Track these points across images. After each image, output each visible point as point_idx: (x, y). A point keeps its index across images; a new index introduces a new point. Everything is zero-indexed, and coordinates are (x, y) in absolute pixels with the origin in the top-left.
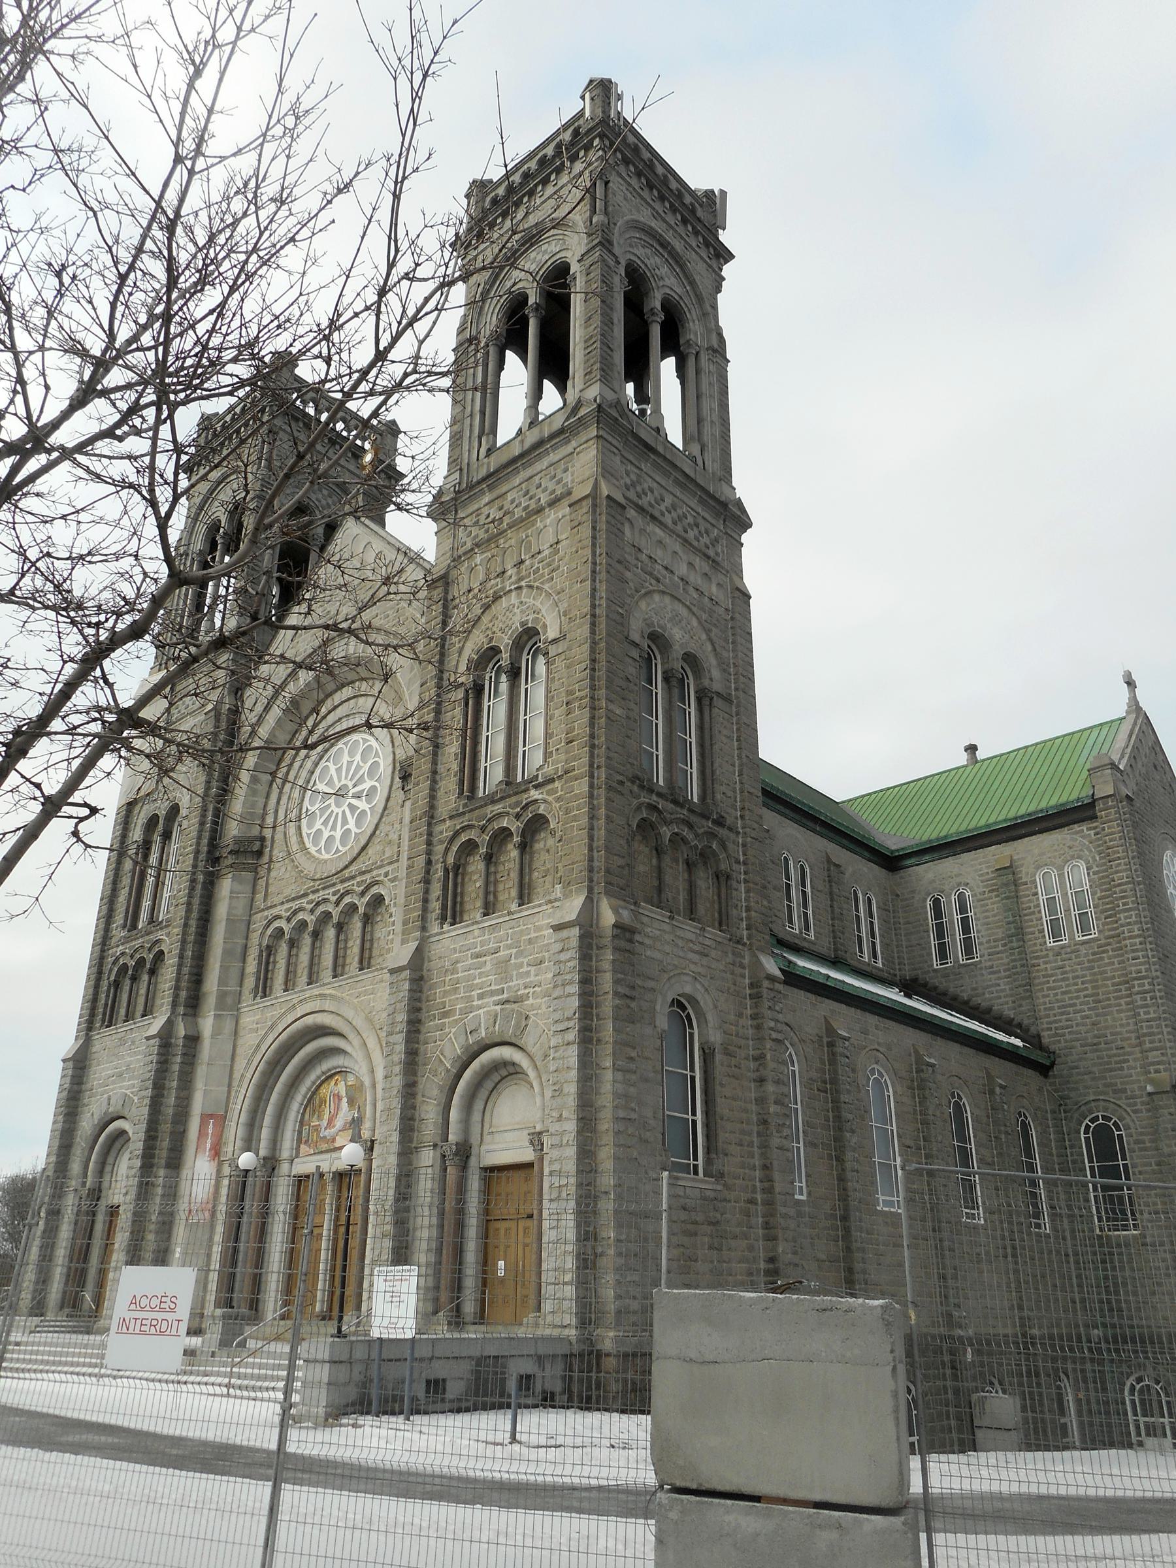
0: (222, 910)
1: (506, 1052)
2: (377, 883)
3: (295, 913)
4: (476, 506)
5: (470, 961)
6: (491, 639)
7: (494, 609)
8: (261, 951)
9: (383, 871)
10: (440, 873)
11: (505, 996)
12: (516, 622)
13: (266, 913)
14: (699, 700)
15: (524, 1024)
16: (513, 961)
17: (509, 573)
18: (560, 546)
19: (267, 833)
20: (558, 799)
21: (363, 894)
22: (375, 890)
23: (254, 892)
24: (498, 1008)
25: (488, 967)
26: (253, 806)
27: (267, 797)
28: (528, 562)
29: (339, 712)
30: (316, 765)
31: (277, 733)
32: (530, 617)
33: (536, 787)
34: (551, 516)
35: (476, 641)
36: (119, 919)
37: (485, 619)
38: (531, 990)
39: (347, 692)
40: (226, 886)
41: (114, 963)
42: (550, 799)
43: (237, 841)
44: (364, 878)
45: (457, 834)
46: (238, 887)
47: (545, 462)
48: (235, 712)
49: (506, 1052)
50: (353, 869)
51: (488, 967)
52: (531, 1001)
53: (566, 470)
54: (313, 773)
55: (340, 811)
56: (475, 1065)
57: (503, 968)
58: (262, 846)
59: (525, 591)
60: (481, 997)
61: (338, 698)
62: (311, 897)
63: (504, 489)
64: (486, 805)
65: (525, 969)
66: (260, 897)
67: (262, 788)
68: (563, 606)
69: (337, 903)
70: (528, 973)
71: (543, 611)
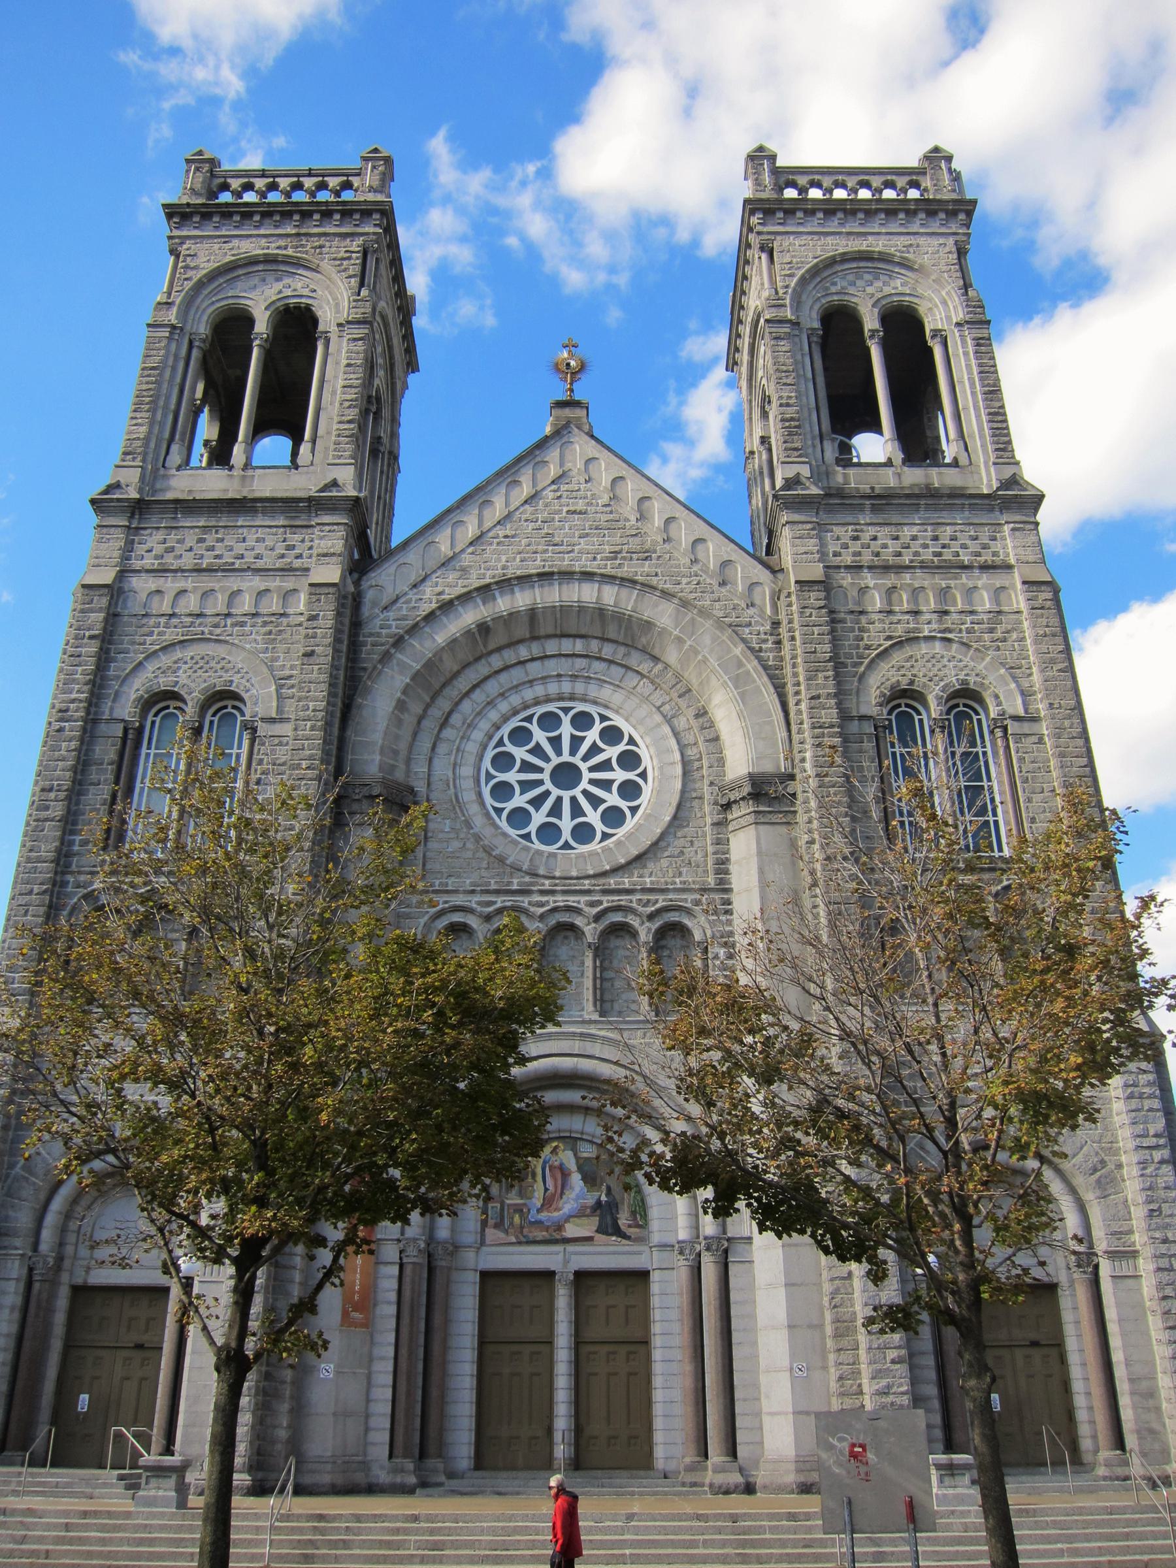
7: (908, 650)
12: (953, 680)
19: (420, 787)
22: (673, 917)
29: (552, 667)
30: (506, 719)
31: (445, 657)
37: (897, 657)
39: (567, 646)
44: (652, 897)
53: (994, 539)
54: (498, 728)
61: (551, 647)
62: (537, 898)
67: (409, 720)
69: (597, 918)
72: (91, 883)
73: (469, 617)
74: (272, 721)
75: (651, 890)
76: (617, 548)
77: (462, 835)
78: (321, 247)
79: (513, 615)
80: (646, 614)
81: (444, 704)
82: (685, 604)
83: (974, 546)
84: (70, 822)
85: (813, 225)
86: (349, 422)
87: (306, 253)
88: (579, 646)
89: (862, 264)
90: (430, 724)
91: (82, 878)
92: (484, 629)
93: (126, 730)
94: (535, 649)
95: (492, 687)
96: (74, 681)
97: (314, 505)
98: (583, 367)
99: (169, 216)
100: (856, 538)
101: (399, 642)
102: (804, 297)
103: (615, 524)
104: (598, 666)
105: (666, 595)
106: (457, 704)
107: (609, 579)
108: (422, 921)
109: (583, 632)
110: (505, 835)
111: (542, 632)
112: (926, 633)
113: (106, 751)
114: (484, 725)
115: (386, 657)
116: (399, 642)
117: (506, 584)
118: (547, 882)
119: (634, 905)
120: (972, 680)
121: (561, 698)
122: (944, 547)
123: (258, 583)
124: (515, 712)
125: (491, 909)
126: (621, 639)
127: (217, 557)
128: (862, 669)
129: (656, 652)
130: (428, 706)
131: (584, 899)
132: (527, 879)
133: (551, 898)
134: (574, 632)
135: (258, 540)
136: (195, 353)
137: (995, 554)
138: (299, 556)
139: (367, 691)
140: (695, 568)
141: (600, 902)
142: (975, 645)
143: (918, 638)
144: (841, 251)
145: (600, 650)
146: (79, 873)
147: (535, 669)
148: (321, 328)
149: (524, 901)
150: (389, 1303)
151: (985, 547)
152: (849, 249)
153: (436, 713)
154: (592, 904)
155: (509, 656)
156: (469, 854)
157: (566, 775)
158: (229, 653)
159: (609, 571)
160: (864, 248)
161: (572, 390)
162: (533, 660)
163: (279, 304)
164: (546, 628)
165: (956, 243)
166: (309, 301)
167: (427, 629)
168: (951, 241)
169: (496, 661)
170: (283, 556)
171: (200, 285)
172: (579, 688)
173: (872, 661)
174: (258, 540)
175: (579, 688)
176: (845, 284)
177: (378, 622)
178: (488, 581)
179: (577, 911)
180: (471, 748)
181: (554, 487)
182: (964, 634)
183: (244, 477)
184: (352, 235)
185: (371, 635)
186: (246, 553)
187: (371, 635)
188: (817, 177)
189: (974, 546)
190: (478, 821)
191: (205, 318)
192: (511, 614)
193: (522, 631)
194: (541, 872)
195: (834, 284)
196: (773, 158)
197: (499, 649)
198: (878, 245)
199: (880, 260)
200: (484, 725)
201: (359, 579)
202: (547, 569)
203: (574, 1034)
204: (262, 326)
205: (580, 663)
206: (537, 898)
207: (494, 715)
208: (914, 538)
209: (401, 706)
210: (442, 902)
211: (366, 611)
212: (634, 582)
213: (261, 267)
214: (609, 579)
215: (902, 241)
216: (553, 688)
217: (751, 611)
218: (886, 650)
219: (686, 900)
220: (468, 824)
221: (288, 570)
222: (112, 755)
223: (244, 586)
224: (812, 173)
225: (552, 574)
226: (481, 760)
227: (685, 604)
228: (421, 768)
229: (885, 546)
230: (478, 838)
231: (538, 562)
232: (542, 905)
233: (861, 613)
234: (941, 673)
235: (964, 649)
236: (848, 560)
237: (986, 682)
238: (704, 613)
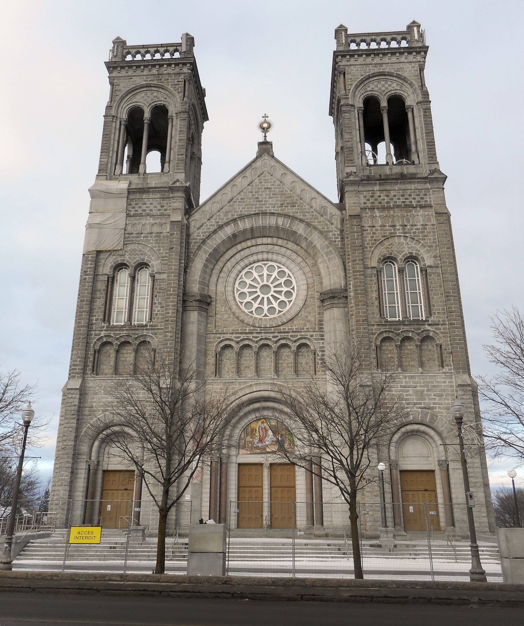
1: (423, 428)
2: (306, 338)
3: (243, 340)
4: (371, 189)
5: (400, 389)
6: (391, 254)
7: (391, 241)
9: (309, 334)
10: (374, 348)
11: (423, 406)
12: (406, 251)
13: (218, 335)
15: (436, 418)
16: (425, 392)
17: (398, 227)
18: (427, 227)
19: (213, 296)
20: (442, 333)
21: (295, 341)
22: (303, 341)
24: (420, 410)
25: (411, 392)
26: (204, 278)
27: (210, 276)
28: (409, 227)
29: (260, 248)
30: (243, 269)
33: (429, 325)
34: (421, 212)
36: (98, 314)
37: (386, 243)
38: (438, 406)
39: (265, 240)
40: (194, 316)
41: (98, 340)
42: (438, 332)
43: (201, 295)
44: (296, 334)
45: (382, 332)
46: (201, 319)
47: (413, 186)
48: (188, 227)
49: (423, 428)
50: (286, 328)
51: (411, 392)
52: (437, 410)
53: (426, 195)
54: (241, 272)
55: (265, 297)
56: (403, 430)
57: (420, 394)
59: (409, 239)
61: (259, 241)
62: (255, 335)
63: (388, 188)
64: (399, 325)
65: (433, 397)
66: (211, 327)
67: (208, 271)
70: (435, 399)
71: (422, 251)
72: (101, 334)
73: (229, 230)
74: (160, 273)
75: (295, 332)
76: (283, 202)
77: (229, 313)
78: (168, 80)
79: (245, 230)
80: (294, 228)
81: (220, 264)
82: (308, 224)
83: (418, 198)
84: (91, 312)
85: (361, 60)
86: (182, 155)
87: (162, 82)
88: (269, 240)
89: (380, 77)
90: (216, 271)
91: (97, 332)
92: (234, 236)
93: (108, 278)
94: (253, 242)
95: (238, 257)
96: (89, 260)
97: (172, 189)
98: (270, 126)
99: (108, 68)
100: (372, 197)
101: (204, 242)
102: (357, 93)
103: (282, 194)
104: (276, 248)
105: (301, 221)
106: (225, 264)
107: (279, 215)
108: (215, 344)
109: (271, 235)
110: (244, 312)
111: (256, 236)
112: (398, 234)
113: (101, 286)
114: (235, 271)
115: (199, 248)
116: (204, 242)
117: (242, 217)
118: (259, 329)
119: (289, 337)
120: (414, 252)
121: (263, 260)
122: (406, 199)
123: (151, 221)
124: (247, 266)
125: (239, 339)
126: (285, 238)
127: (136, 211)
128: (373, 249)
129: (298, 242)
130: (215, 265)
131: (271, 335)
132: (252, 328)
133: (260, 335)
134: (268, 235)
135: (151, 204)
136: (122, 127)
137: (427, 201)
138: (166, 210)
139: (193, 260)
140: (312, 210)
141: (278, 336)
142: (416, 238)
143: (395, 236)
144: (372, 72)
145: (277, 242)
146: (96, 330)
147: (253, 249)
148: (170, 114)
149: (251, 336)
150: (208, 475)
151: (422, 198)
152: (376, 71)
153: (218, 267)
154: (274, 337)
155: (244, 245)
156: (231, 319)
157: (265, 288)
158: (143, 248)
159: (280, 211)
160: (381, 70)
161: (265, 136)
162: (252, 246)
163: (153, 104)
164: (256, 234)
165: (419, 65)
166: (165, 103)
167: (214, 236)
168: (417, 65)
169: (239, 247)
170: (160, 210)
171: (123, 98)
172: (270, 256)
173: (377, 246)
174: (151, 204)
175: (270, 256)
176: (373, 86)
177: (196, 234)
178: (235, 216)
179: (270, 339)
180: (231, 280)
181: (259, 178)
182: (412, 234)
183: (144, 178)
184: (179, 74)
185: (194, 239)
186: (147, 209)
187: (194, 239)
188: (364, 38)
189: (418, 198)
190: (234, 307)
191: (125, 111)
192: (244, 230)
193: (249, 236)
194: (257, 325)
195: (369, 87)
196: (346, 30)
197: (240, 243)
198: (387, 69)
199: (387, 75)
200: (235, 271)
201: (189, 218)
202: (257, 212)
203: (269, 383)
204: (147, 115)
205: (270, 247)
206: (255, 335)
207: (239, 267)
208: (395, 196)
209: (205, 266)
211: (192, 229)
212: (289, 216)
213: (145, 89)
214: (279, 215)
215: (396, 66)
216: (260, 257)
217: (333, 226)
218: (382, 241)
219: (307, 335)
220: (230, 308)
221: (162, 215)
222: (104, 287)
223: (147, 222)
224: (362, 36)
225: (259, 213)
226: (235, 284)
227: (308, 224)
228: (212, 288)
229: (384, 199)
230: (234, 314)
231: (254, 209)
232: (256, 337)
233: (373, 227)
234: (402, 250)
235: (412, 240)
236: (369, 205)
237: (419, 253)
238: (315, 228)
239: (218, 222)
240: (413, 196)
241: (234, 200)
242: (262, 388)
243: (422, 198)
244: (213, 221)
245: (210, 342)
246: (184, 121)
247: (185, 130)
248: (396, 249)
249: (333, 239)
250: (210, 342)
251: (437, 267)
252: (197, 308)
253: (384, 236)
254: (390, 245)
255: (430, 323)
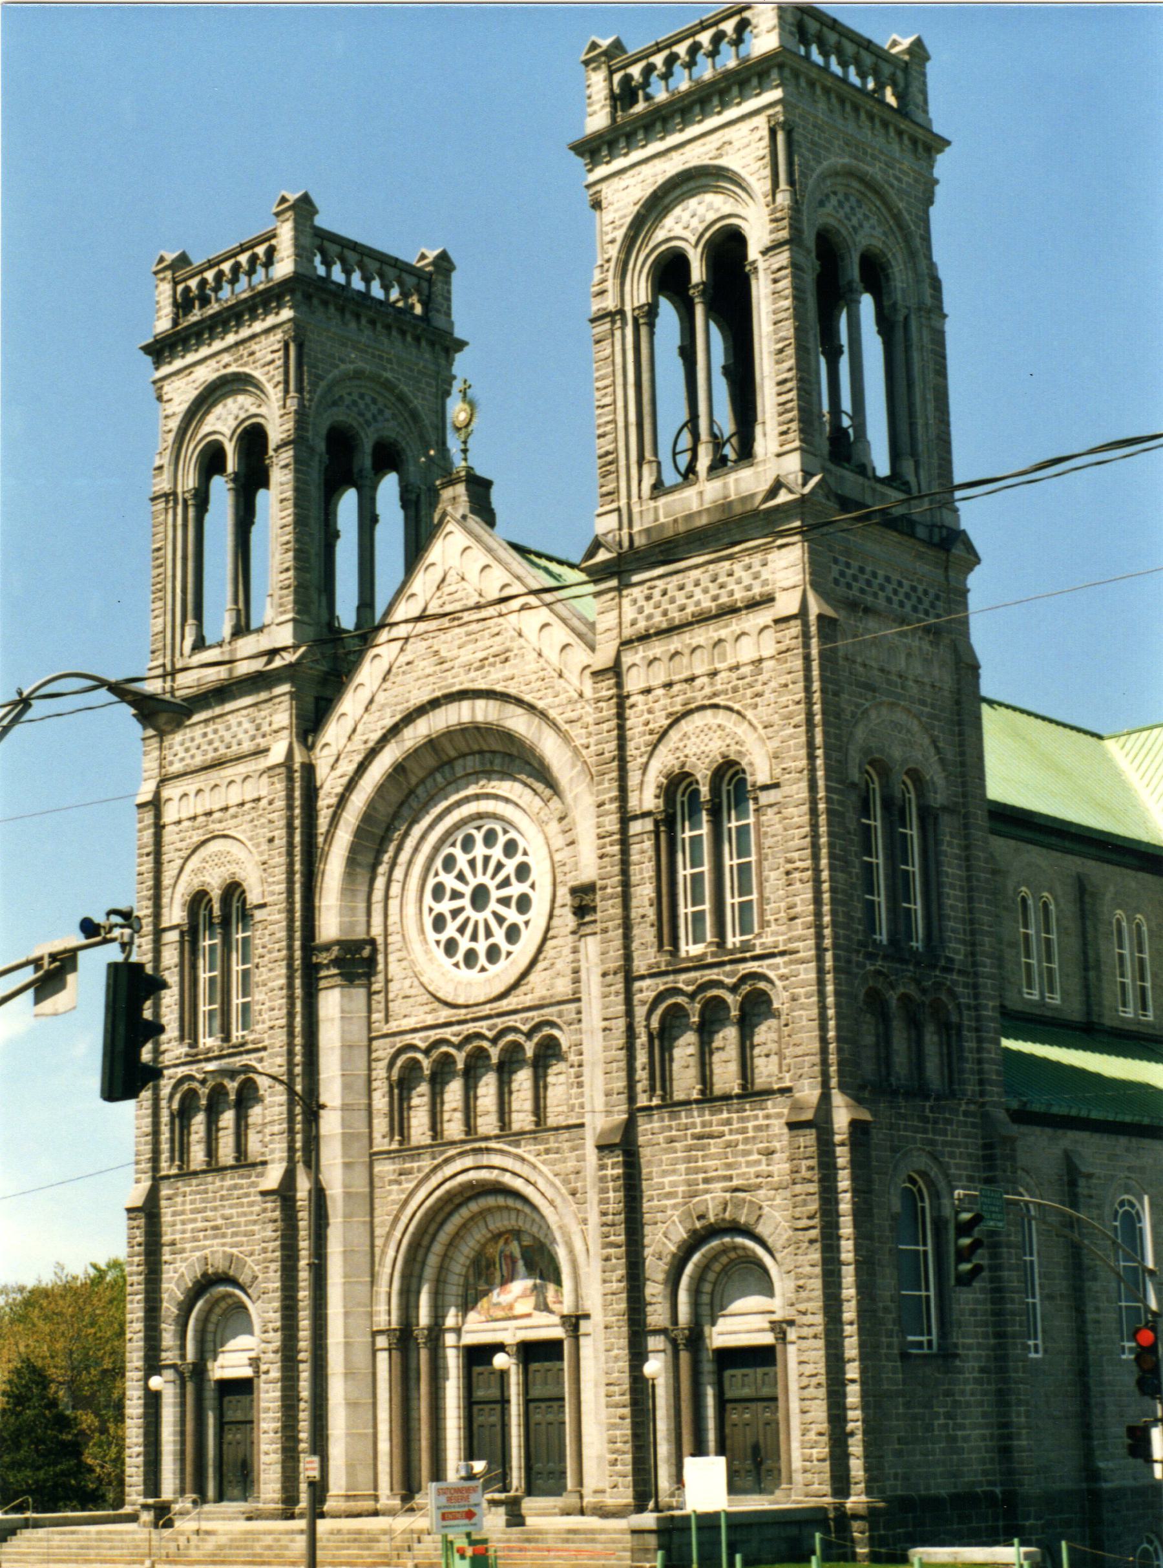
0: (330, 1036)
8: (391, 1088)
14: (922, 819)
18: (765, 664)
22: (547, 1031)
23: (370, 1011)
24: (728, 1195)
32: (734, 748)
35: (664, 761)
37: (674, 735)
48: (309, 769)
58: (375, 951)
60: (706, 1181)
65: (755, 1157)
68: (772, 745)
70: (758, 1162)
86: (287, 570)
100: (648, 598)
137: (765, 583)
210: (400, 1042)
239: (366, 742)
240: (736, 575)
241: (394, 670)
242: (458, 1165)
243: (756, 576)
244: (357, 738)
245: (378, 1060)
246: (286, 471)
247: (289, 494)
248: (694, 749)
249: (584, 741)
250: (378, 1060)
251: (776, 786)
252: (338, 980)
253: (671, 714)
254: (681, 740)
255: (758, 951)
